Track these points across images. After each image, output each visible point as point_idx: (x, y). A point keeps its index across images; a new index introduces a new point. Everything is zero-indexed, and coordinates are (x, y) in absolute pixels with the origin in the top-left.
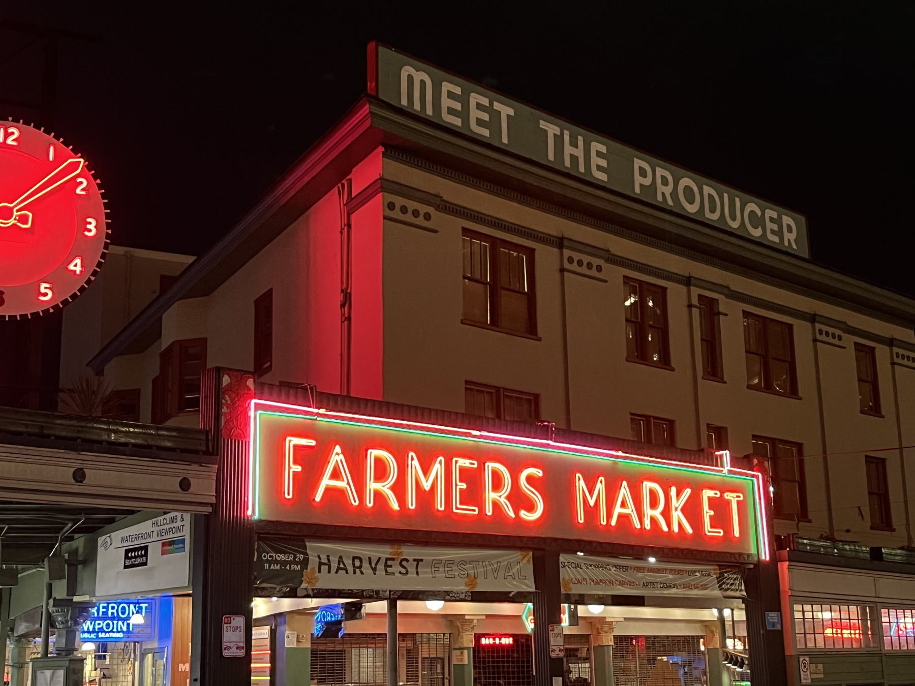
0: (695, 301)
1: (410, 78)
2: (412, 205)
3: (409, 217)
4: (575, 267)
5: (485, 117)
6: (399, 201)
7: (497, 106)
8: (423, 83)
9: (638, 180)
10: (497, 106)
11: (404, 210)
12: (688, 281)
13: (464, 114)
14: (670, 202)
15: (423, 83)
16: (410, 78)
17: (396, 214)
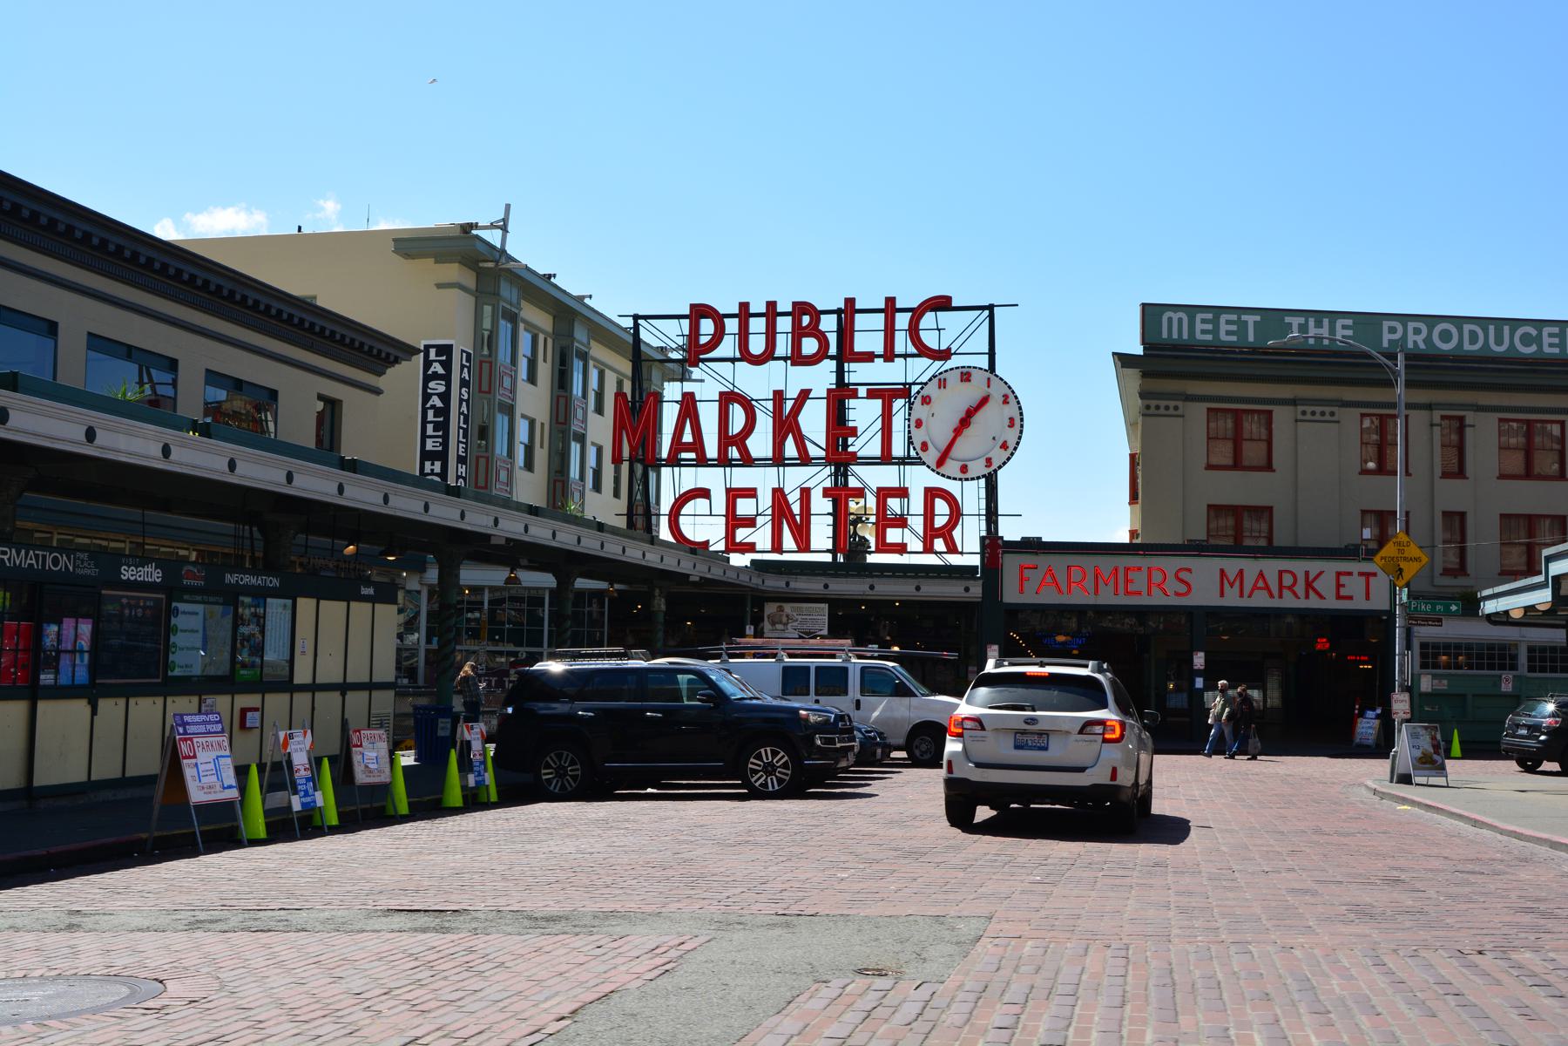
0: (1437, 419)
1: (1170, 320)
2: (1163, 403)
3: (1162, 411)
4: (1308, 417)
5: (1234, 328)
6: (1153, 403)
7: (1244, 317)
8: (1180, 320)
9: (1386, 337)
10: (1244, 317)
11: (1158, 407)
12: (1429, 407)
13: (1215, 331)
14: (1422, 346)
15: (1180, 320)
16: (1170, 320)
17: (1153, 410)
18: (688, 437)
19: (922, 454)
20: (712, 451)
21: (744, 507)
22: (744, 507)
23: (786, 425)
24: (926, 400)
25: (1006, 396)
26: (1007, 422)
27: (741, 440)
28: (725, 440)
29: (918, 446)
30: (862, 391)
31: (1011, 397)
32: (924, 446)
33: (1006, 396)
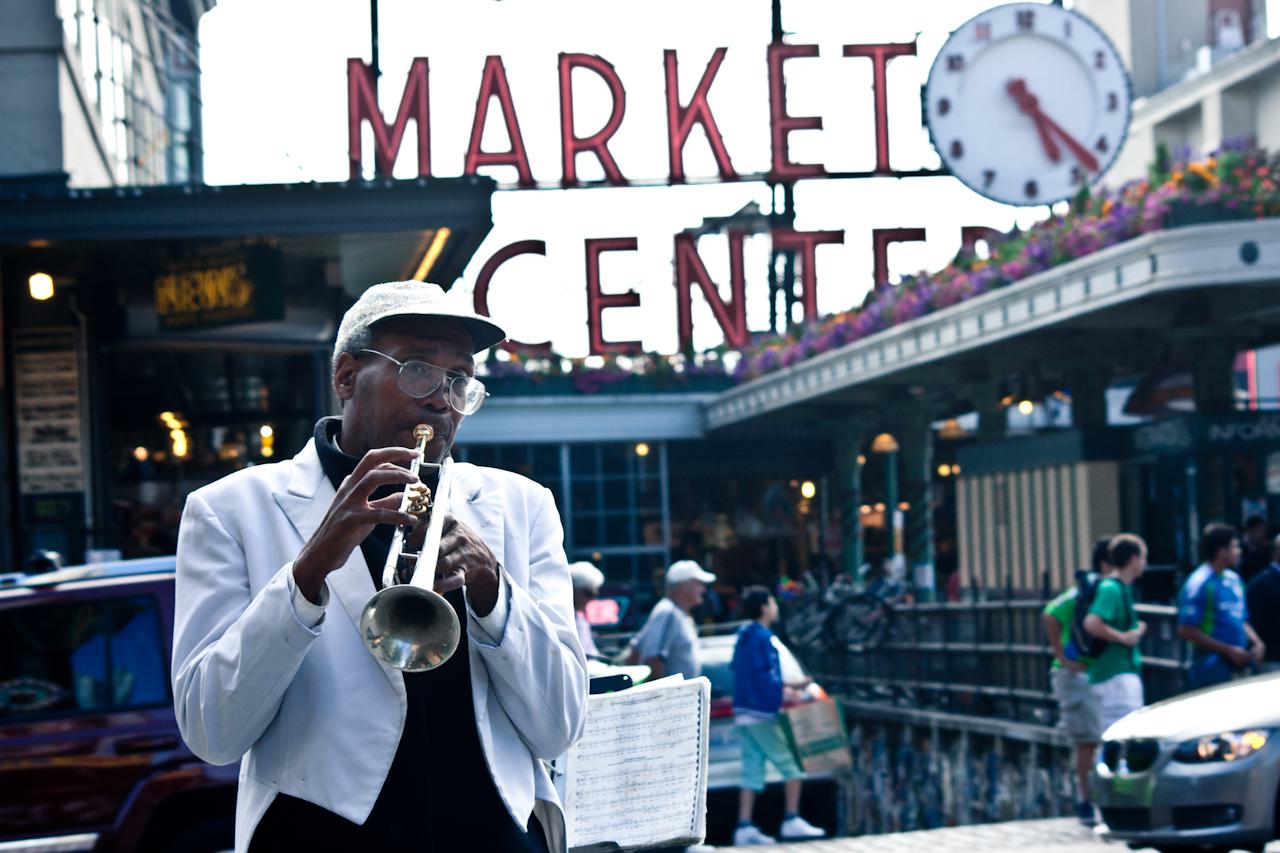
18: (496, 140)
19: (953, 164)
20: (546, 162)
21: (615, 273)
22: (615, 273)
23: (686, 116)
24: (955, 63)
25: (1100, 55)
26: (1104, 102)
27: (598, 145)
28: (572, 146)
29: (946, 148)
30: (831, 50)
31: (1109, 59)
32: (957, 149)
33: (1100, 55)
